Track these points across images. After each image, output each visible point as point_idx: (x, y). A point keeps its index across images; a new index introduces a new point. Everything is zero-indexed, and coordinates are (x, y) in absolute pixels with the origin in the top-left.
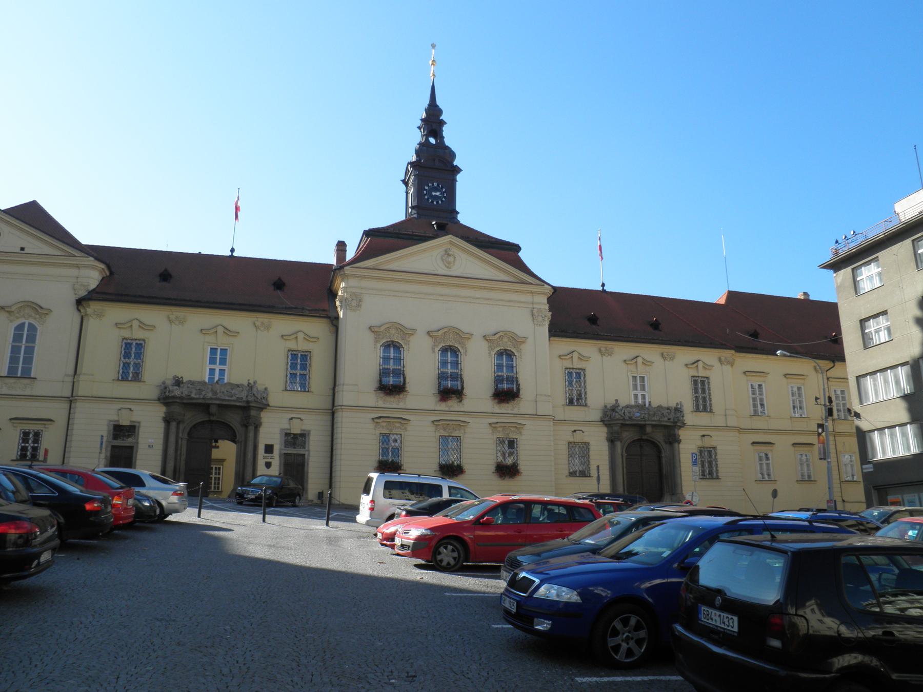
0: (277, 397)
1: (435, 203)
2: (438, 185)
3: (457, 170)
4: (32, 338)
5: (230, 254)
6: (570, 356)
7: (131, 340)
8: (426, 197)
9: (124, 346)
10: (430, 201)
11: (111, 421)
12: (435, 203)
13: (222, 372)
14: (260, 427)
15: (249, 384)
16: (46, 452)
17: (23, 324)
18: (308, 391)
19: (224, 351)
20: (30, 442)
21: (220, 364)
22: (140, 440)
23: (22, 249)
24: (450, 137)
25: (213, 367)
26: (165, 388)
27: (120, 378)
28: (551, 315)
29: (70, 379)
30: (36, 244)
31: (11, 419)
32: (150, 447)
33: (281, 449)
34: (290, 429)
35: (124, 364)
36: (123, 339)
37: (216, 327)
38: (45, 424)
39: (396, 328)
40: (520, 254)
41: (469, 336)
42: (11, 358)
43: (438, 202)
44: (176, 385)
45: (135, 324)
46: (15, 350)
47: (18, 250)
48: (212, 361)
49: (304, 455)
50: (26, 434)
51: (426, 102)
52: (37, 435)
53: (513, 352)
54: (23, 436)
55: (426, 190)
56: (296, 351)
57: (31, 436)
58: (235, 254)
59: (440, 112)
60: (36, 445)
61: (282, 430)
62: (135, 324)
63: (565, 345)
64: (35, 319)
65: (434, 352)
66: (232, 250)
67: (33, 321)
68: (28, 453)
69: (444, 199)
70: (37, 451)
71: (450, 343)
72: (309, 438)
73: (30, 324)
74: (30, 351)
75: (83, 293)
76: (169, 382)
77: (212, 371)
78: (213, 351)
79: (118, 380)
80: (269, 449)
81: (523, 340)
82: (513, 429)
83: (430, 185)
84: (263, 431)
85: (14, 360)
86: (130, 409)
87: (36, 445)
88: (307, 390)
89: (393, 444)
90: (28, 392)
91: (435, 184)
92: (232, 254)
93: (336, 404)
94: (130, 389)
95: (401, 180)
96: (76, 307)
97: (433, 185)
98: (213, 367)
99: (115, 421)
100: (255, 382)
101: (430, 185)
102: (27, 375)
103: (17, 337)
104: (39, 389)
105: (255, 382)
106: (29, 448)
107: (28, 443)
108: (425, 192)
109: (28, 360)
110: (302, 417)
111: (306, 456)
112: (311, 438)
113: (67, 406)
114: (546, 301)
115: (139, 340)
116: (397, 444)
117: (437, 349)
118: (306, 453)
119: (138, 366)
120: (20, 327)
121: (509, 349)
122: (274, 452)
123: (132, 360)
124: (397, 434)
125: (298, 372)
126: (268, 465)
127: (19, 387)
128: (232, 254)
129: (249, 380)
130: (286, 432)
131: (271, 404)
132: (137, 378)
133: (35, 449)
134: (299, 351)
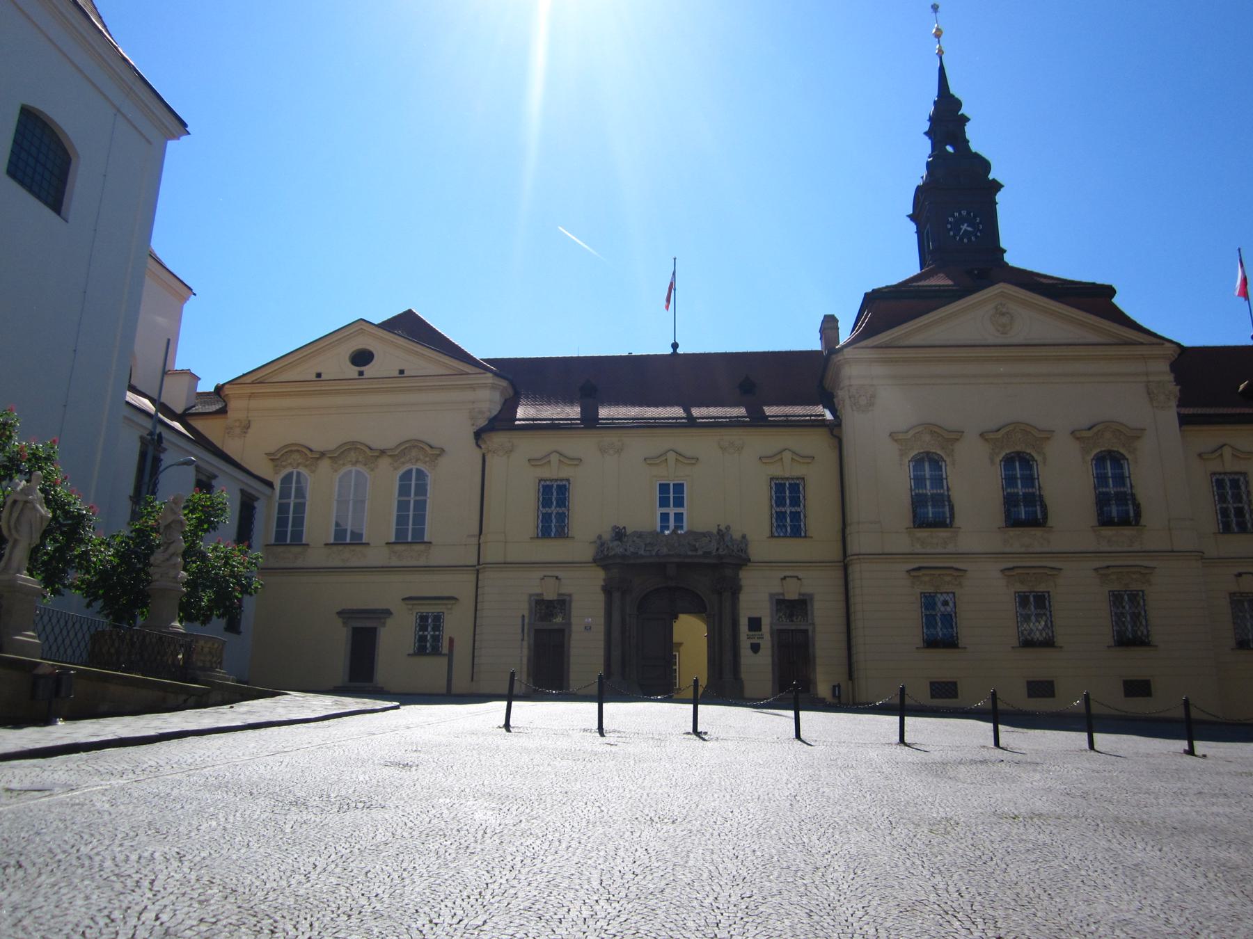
0: (762, 544)
1: (965, 240)
2: (968, 214)
3: (996, 186)
4: (421, 489)
5: (672, 350)
6: (1217, 454)
7: (551, 480)
8: (951, 233)
9: (541, 490)
11: (531, 595)
13: (679, 517)
14: (739, 593)
15: (719, 530)
16: (451, 641)
17: (410, 471)
18: (805, 537)
19: (679, 488)
20: (429, 629)
21: (674, 506)
22: (574, 620)
23: (402, 372)
24: (978, 139)
25: (664, 510)
26: (602, 544)
27: (540, 535)
28: (1180, 391)
29: (475, 541)
30: (420, 361)
31: (403, 599)
32: (588, 628)
33: (771, 624)
34: (783, 594)
35: (544, 515)
36: (540, 481)
37: (665, 453)
38: (446, 604)
39: (932, 433)
40: (1115, 300)
41: (1047, 435)
42: (399, 517)
44: (616, 540)
45: (554, 458)
46: (403, 506)
47: (396, 374)
48: (664, 502)
49: (806, 631)
50: (423, 618)
51: (933, 94)
52: (438, 618)
53: (1122, 454)
54: (421, 621)
55: (951, 223)
56: (782, 479)
57: (430, 621)
58: (680, 351)
59: (958, 104)
60: (437, 633)
61: (771, 595)
62: (554, 458)
63: (1208, 437)
64: (425, 463)
65: (992, 461)
66: (675, 346)
67: (420, 466)
68: (428, 645)
69: (979, 234)
70: (439, 641)
71: (1018, 449)
72: (812, 606)
73: (418, 471)
74: (421, 506)
75: (482, 423)
76: (607, 536)
77: (665, 517)
78: (664, 488)
79: (538, 537)
80: (755, 624)
81: (1135, 435)
82: (1134, 576)
83: (957, 214)
84: (744, 597)
85: (402, 520)
86: (557, 578)
87: (437, 633)
88: (803, 534)
89: (942, 609)
90: (422, 562)
91: (964, 213)
93: (849, 552)
94: (552, 550)
95: (908, 216)
96: (474, 441)
97: (960, 214)
98: (664, 510)
99: (537, 595)
100: (728, 528)
101: (957, 214)
102: (419, 538)
103: (404, 490)
104: (437, 557)
105: (728, 528)
106: (429, 637)
107: (427, 630)
108: (949, 226)
109: (420, 519)
110: (800, 575)
111: (810, 633)
112: (817, 605)
113: (473, 577)
114: (1168, 369)
115: (561, 480)
116: (949, 609)
117: (998, 459)
118: (810, 628)
119: (562, 518)
120: (406, 476)
121: (1115, 449)
122: (763, 627)
124: (947, 593)
126: (755, 648)
127: (410, 556)
129: (719, 526)
130: (777, 597)
131: (752, 558)
132: (562, 534)
133: (436, 639)
134: (787, 479)
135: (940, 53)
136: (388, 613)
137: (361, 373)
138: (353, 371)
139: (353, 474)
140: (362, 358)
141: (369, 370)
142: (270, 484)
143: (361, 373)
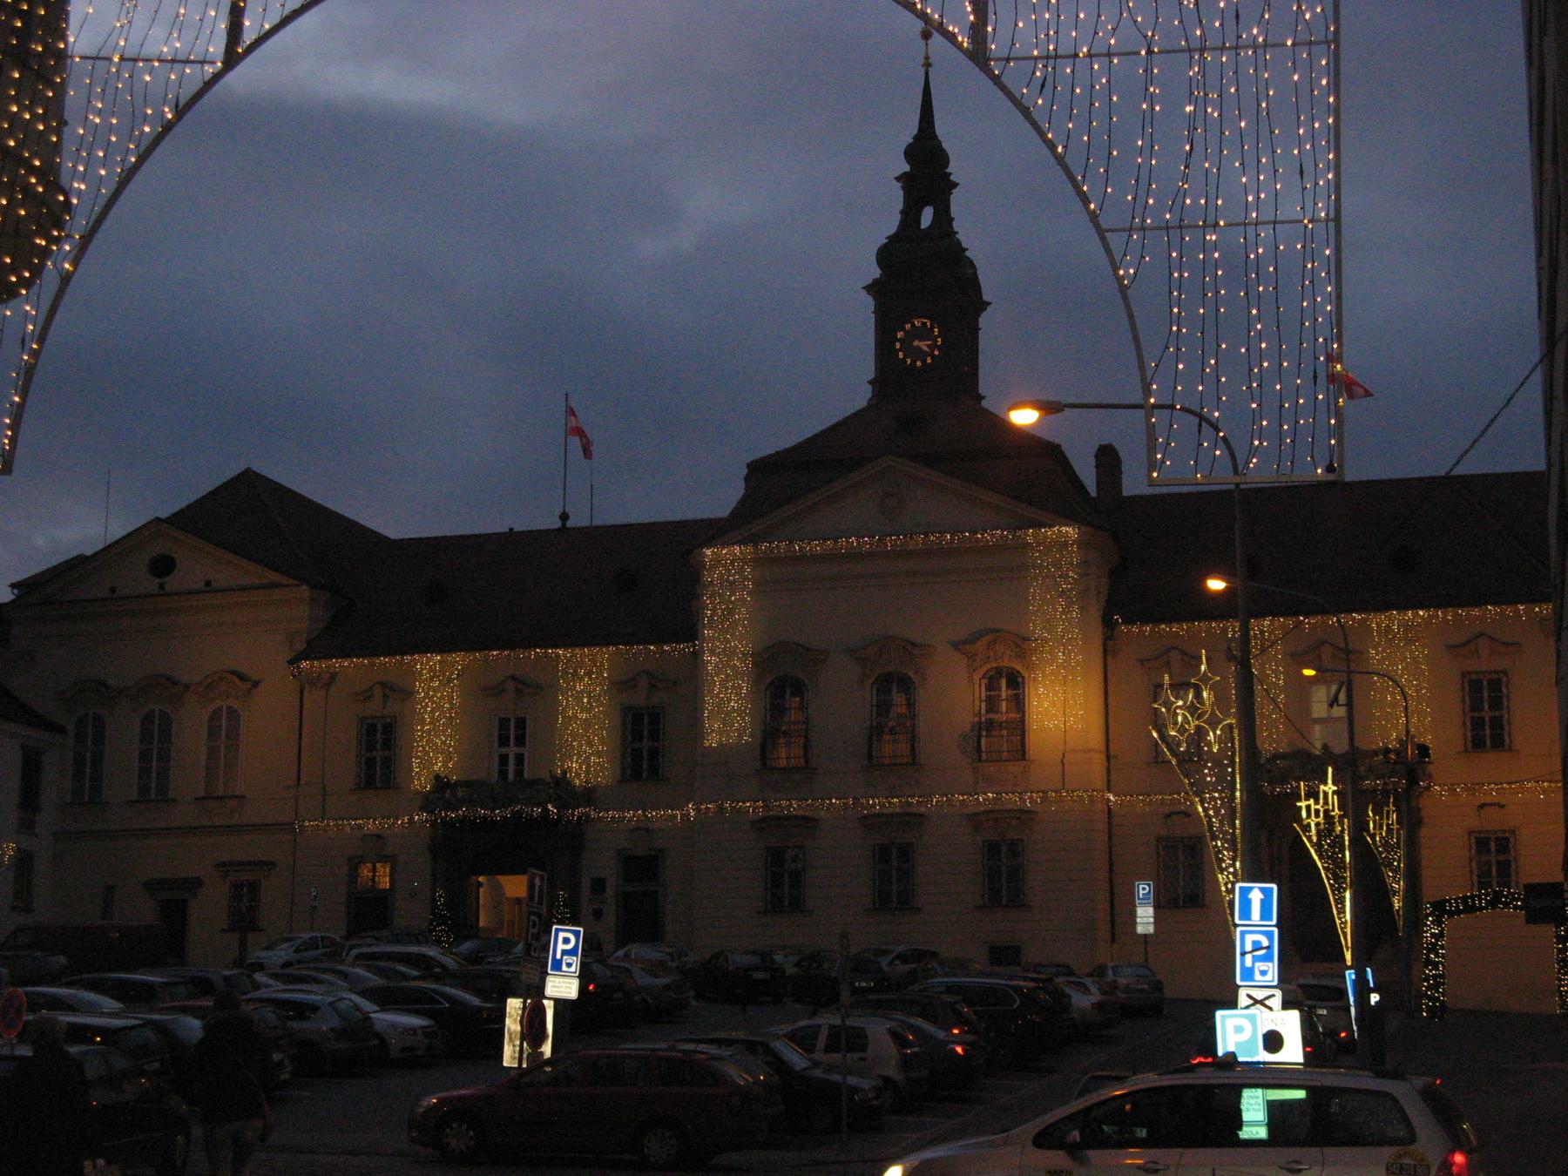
10: (909, 361)
12: (919, 364)
13: (520, 759)
15: (553, 777)
17: (220, 710)
19: (521, 723)
25: (504, 750)
43: (924, 361)
47: (202, 585)
52: (254, 887)
58: (569, 524)
66: (564, 517)
67: (230, 702)
73: (229, 708)
77: (504, 759)
78: (504, 723)
80: (599, 885)
82: (1014, 822)
92: (564, 525)
122: (608, 890)
123: (379, 754)
125: (646, 744)
128: (564, 525)
135: (927, 65)
136: (198, 883)
137: (162, 586)
138: (151, 584)
139: (157, 715)
140: (162, 566)
141: (173, 582)
142: (62, 730)
143: (162, 586)
